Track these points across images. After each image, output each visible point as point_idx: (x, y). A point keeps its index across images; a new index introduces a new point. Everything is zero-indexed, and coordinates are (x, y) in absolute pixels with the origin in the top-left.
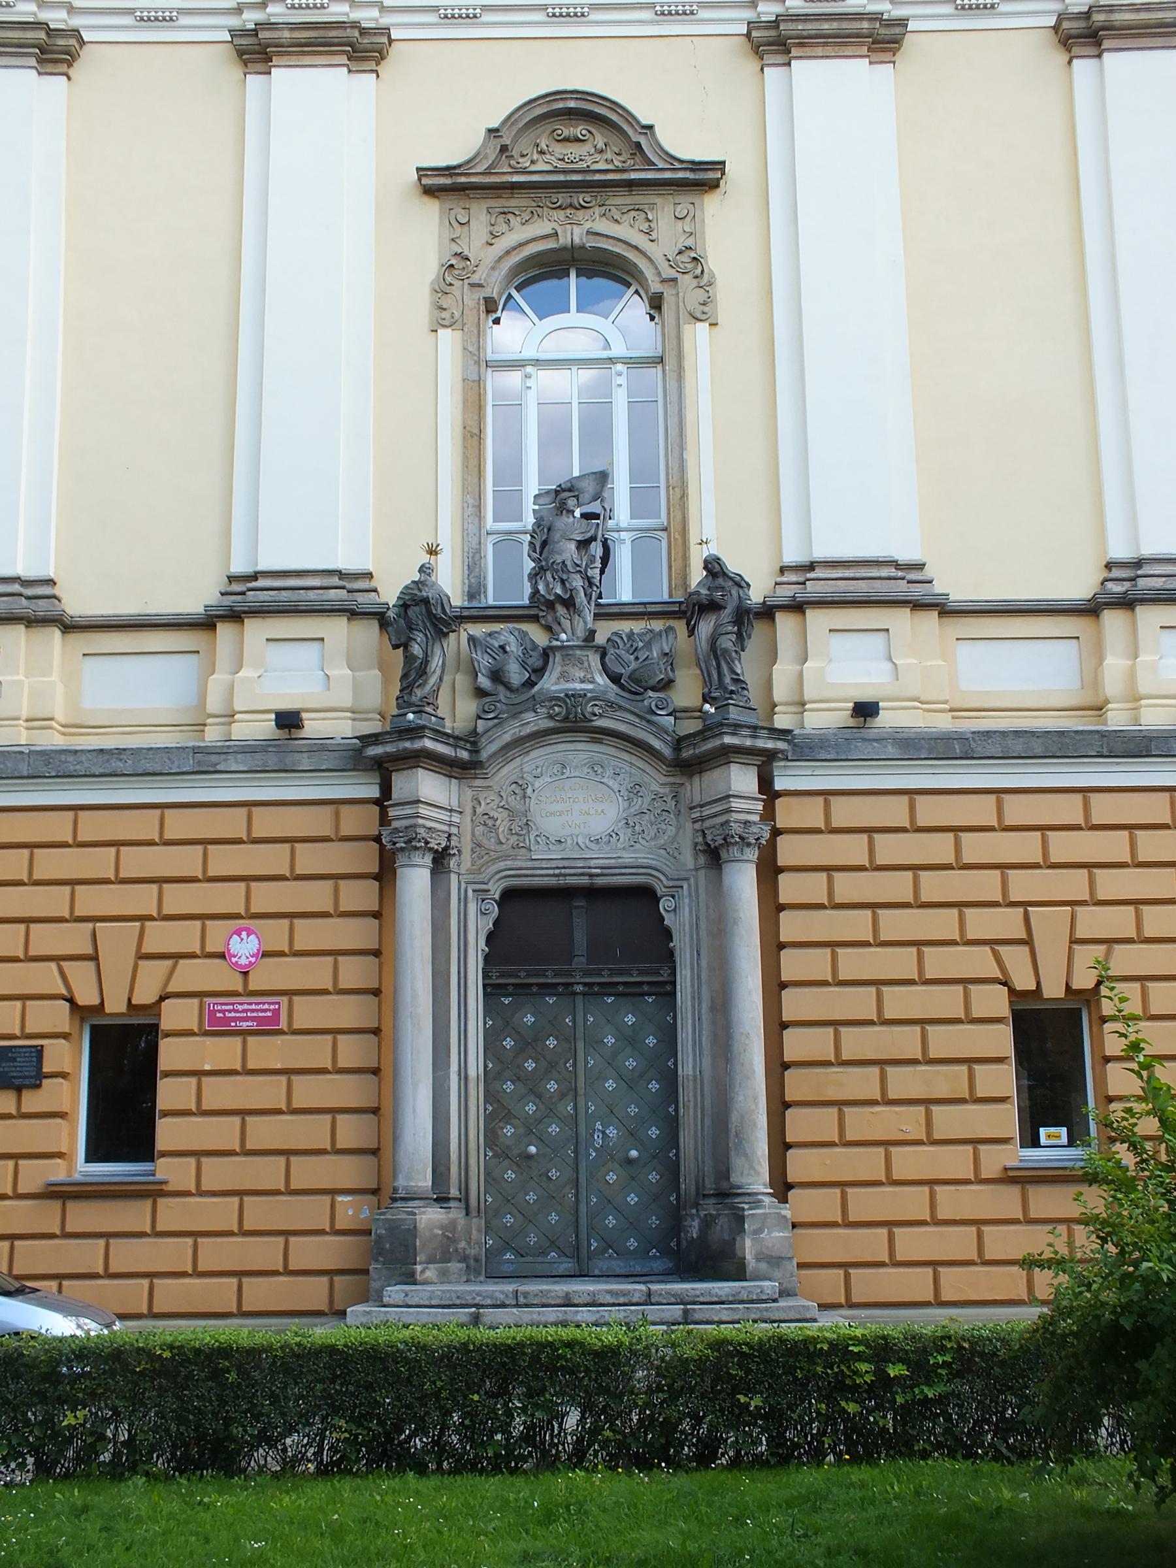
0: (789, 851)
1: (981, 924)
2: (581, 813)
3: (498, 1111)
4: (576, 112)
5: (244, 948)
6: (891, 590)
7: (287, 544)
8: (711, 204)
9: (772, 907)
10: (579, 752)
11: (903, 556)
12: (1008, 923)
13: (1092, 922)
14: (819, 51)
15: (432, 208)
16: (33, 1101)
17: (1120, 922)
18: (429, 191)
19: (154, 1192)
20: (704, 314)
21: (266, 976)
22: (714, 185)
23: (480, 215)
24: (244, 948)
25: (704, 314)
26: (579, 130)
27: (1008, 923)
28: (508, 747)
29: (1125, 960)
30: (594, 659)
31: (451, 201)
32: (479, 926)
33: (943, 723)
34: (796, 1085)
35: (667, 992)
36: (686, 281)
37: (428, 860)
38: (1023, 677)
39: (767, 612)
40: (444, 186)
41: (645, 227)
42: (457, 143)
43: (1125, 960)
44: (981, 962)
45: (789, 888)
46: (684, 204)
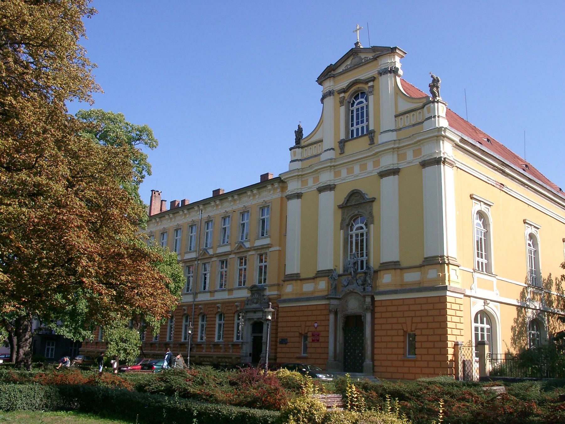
0: (377, 309)
2: (353, 306)
3: (346, 348)
4: (355, 194)
6: (394, 266)
7: (320, 268)
9: (373, 318)
19: (415, 361)
20: (372, 223)
21: (319, 329)
22: (373, 201)
24: (316, 325)
25: (372, 223)
26: (357, 195)
29: (419, 326)
39: (376, 272)
40: (340, 207)
42: (341, 201)
43: (419, 326)
45: (377, 315)
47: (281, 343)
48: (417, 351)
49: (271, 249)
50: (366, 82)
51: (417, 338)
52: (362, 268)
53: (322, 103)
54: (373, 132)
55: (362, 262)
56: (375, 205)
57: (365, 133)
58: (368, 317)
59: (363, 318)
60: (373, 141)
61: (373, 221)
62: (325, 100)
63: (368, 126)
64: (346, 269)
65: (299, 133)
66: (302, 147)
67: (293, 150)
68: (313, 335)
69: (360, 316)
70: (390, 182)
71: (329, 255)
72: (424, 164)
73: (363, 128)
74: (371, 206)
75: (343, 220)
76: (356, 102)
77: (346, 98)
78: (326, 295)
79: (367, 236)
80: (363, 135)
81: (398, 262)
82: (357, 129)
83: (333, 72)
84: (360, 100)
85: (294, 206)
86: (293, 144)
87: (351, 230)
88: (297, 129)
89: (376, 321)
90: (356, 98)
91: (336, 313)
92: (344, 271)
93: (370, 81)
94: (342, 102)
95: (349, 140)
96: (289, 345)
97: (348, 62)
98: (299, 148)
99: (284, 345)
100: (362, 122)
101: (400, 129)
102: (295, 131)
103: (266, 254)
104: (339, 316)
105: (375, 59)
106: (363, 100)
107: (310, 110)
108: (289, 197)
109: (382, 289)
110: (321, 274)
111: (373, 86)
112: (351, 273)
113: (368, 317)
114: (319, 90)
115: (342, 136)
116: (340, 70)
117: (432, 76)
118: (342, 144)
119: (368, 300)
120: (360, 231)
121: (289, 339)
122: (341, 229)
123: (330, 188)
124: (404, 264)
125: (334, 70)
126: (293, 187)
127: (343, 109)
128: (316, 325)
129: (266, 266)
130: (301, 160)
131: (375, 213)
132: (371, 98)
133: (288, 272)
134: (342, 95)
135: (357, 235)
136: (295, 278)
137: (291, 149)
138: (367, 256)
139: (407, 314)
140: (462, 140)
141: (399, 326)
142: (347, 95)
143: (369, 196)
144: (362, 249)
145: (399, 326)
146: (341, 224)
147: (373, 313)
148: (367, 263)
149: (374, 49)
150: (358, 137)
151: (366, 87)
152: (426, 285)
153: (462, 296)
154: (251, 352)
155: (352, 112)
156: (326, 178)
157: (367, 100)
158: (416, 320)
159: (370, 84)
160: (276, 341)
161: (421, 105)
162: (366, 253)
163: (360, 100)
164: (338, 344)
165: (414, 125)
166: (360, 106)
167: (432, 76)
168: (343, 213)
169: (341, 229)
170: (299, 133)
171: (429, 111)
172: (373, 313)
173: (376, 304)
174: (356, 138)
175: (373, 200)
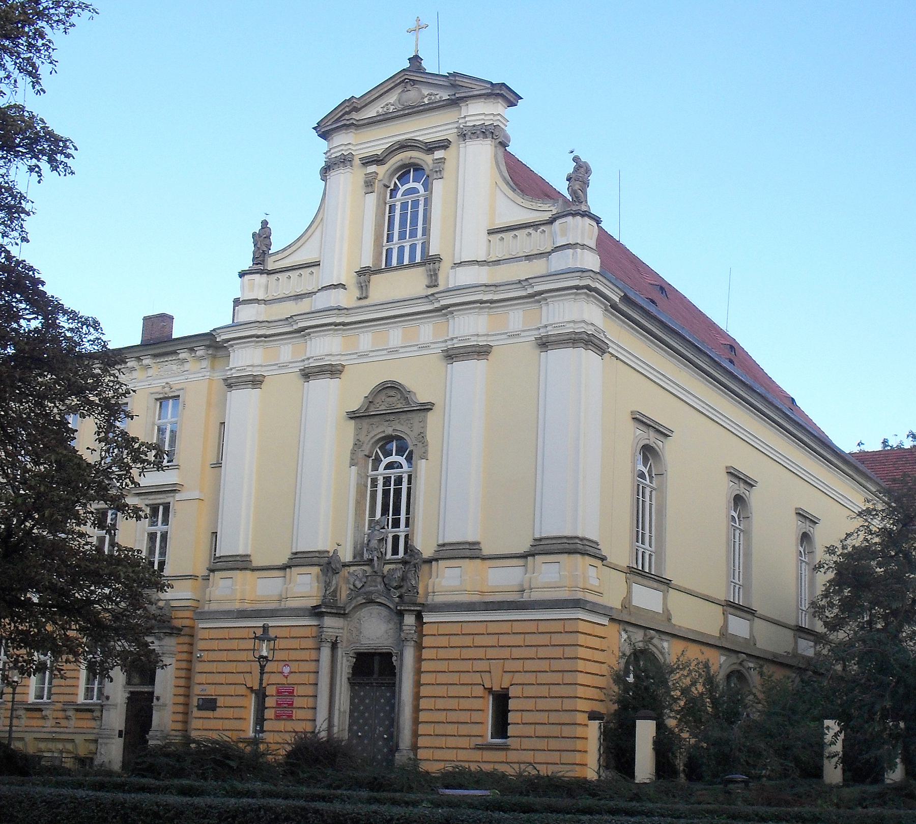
0: (426, 641)
2: (374, 630)
4: (390, 388)
5: (286, 670)
6: (468, 551)
8: (430, 414)
9: (419, 659)
10: (375, 609)
11: (470, 540)
14: (461, 358)
15: (353, 422)
18: (351, 418)
20: (424, 456)
23: (365, 423)
25: (424, 456)
26: (392, 393)
28: (354, 608)
29: (518, 678)
30: (379, 579)
31: (357, 420)
33: (476, 598)
36: (420, 445)
37: (329, 645)
38: (502, 579)
39: (429, 561)
40: (353, 416)
41: (409, 425)
45: (426, 654)
46: (422, 414)
47: (200, 708)
48: (511, 730)
49: (178, 496)
50: (430, 148)
51: (512, 704)
52: (395, 551)
53: (324, 178)
54: (437, 259)
55: (396, 539)
56: (431, 418)
57: (418, 259)
58: (409, 655)
59: (394, 658)
60: (436, 280)
61: (426, 452)
62: (333, 175)
63: (425, 246)
64: (358, 554)
65: (262, 238)
66: (269, 273)
67: (247, 277)
68: (279, 693)
69: (390, 655)
70: (469, 371)
71: (330, 519)
73: (413, 248)
74: (424, 421)
75: (358, 444)
76: (403, 189)
77: (380, 177)
78: (314, 607)
79: (409, 482)
80: (413, 265)
81: (478, 543)
82: (401, 250)
83: (355, 115)
84: (411, 185)
85: (243, 401)
86: (247, 264)
87: (375, 468)
88: (257, 228)
89: (425, 666)
90: (403, 178)
91: (334, 646)
92: (354, 557)
94: (369, 184)
95: (379, 271)
96: (219, 713)
97: (392, 98)
98: (261, 272)
99: (209, 714)
100: (413, 234)
101: (497, 262)
102: (254, 235)
103: (167, 507)
104: (340, 652)
106: (419, 186)
107: (294, 190)
108: (230, 384)
109: (439, 599)
110: (299, 560)
111: (442, 160)
112: (372, 560)
113: (409, 655)
114: (318, 150)
115: (367, 261)
116: (371, 112)
117: (576, 159)
118: (365, 274)
119: (410, 620)
120: (393, 473)
121: (220, 702)
122: (352, 465)
123: (333, 371)
124: (486, 551)
125: (356, 110)
126: (244, 359)
127: (371, 200)
128: (286, 670)
129: (164, 536)
130: (265, 302)
131: (430, 436)
132: (437, 185)
133: (224, 550)
134: (372, 168)
135: (387, 481)
136: (241, 563)
137: (242, 274)
138: (407, 525)
139: (491, 653)
140: (626, 299)
142: (381, 171)
143: (422, 397)
144: (397, 511)
145: (477, 678)
146: (353, 452)
147: (419, 647)
148: (406, 543)
149: (454, 81)
150: (401, 266)
151: (427, 160)
152: (536, 596)
153: (605, 621)
154: (123, 728)
155: (392, 208)
156: (324, 347)
157: (427, 186)
159: (438, 154)
160: (186, 705)
161: (546, 216)
162: (407, 519)
163: (411, 185)
164: (336, 713)
165: (528, 257)
166: (410, 199)
167: (576, 159)
168: (358, 430)
169: (352, 465)
170: (262, 239)
171: (564, 233)
172: (419, 647)
173: (426, 629)
174: (396, 269)
175: (426, 408)
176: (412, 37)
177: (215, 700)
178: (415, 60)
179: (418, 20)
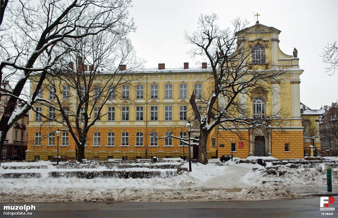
1: (283, 139)
12: (285, 139)
13: (290, 139)
16: (224, 147)
17: (291, 139)
27: (285, 139)
29: (292, 141)
32: (254, 138)
34: (272, 147)
35: (265, 142)
43: (292, 141)
44: (283, 141)
47: (220, 146)
50: (265, 41)
61: (268, 100)
72: (292, 83)
93: (266, 42)
105: (270, 33)
116: (248, 31)
120: (259, 103)
121: (225, 145)
135: (257, 105)
141: (283, 141)
142: (253, 44)
158: (290, 139)
159: (266, 43)
176: (256, 16)
177: (224, 145)
178: (258, 22)
179: (257, 13)
